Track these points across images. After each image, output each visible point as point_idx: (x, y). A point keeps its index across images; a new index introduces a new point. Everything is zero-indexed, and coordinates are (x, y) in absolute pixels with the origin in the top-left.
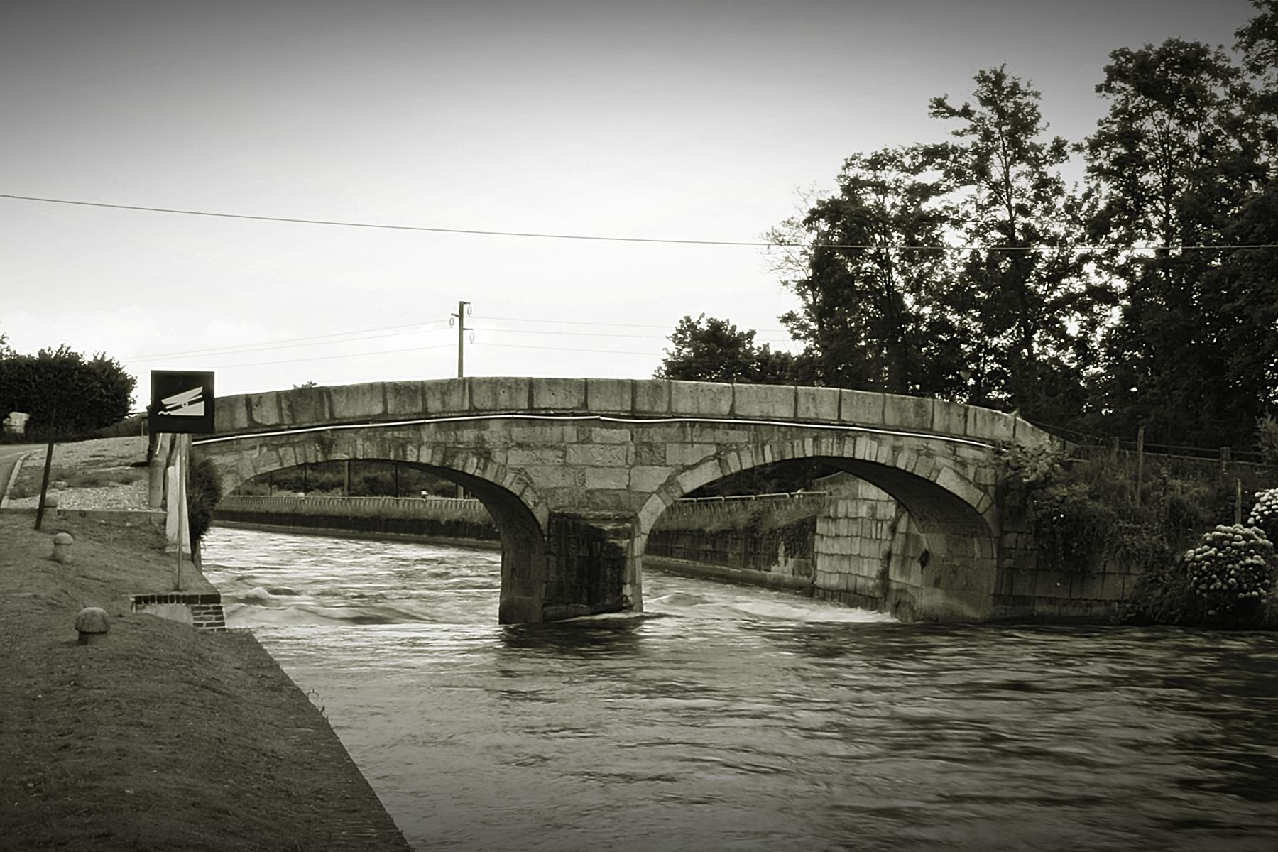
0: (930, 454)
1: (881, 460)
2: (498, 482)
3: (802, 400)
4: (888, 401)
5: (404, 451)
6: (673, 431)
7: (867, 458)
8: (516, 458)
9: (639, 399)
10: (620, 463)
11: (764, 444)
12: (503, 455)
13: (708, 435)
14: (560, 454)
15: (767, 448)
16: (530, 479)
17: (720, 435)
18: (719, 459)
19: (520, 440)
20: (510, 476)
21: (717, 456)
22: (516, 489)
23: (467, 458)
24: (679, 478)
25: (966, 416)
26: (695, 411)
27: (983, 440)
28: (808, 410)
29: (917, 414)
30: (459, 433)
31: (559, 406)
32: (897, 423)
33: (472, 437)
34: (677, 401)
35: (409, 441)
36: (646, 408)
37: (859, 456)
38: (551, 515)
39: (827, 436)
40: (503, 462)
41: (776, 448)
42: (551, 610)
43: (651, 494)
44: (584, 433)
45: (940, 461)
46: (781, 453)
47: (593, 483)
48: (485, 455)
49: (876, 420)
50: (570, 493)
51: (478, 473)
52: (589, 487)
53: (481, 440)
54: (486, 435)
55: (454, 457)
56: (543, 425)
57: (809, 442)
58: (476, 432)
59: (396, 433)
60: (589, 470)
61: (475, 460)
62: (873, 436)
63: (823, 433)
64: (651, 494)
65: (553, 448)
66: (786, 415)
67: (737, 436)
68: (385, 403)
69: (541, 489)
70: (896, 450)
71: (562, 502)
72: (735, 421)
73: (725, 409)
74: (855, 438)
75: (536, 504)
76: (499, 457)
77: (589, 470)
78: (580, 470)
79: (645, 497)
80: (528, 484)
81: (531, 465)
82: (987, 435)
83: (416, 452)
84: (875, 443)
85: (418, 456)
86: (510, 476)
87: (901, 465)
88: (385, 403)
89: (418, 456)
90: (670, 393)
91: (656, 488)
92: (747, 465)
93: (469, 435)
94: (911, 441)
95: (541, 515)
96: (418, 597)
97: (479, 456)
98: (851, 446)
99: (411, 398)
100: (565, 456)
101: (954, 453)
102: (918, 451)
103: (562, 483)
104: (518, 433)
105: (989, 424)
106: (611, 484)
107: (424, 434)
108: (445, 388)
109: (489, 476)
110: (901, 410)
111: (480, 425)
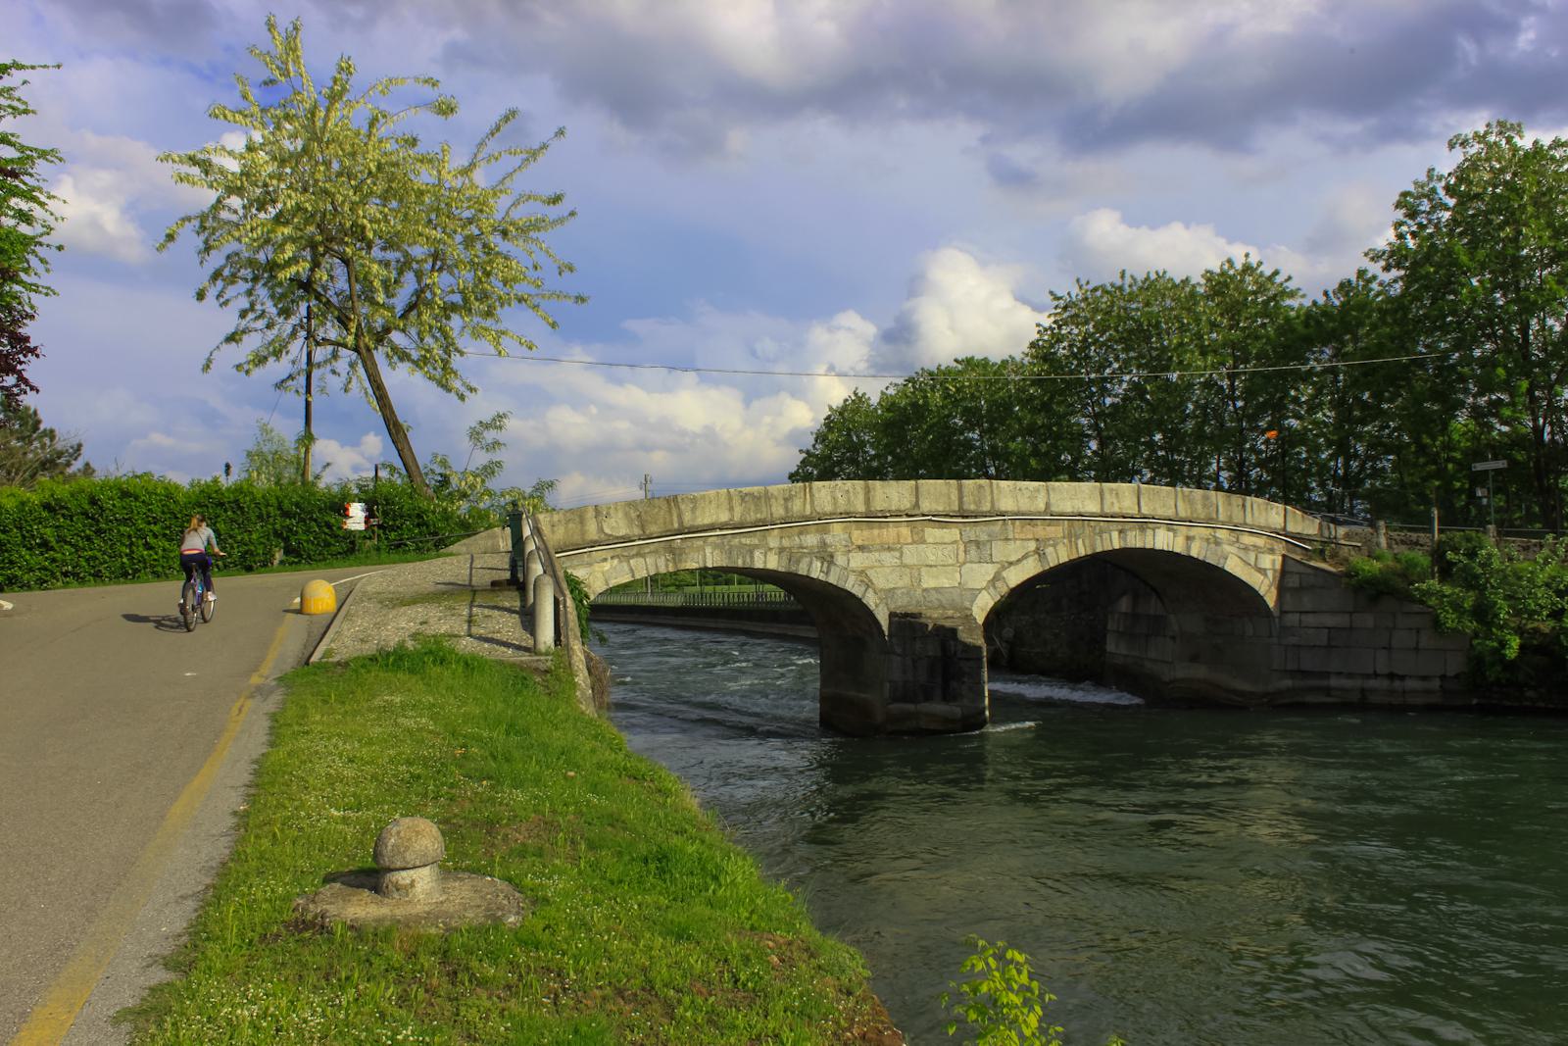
0: (1217, 543)
1: (1177, 550)
2: (841, 585)
3: (1107, 496)
4: (1180, 495)
5: (752, 558)
6: (997, 527)
7: (1166, 549)
8: (858, 560)
9: (965, 499)
10: (950, 561)
11: (1077, 538)
12: (845, 558)
13: (1029, 531)
14: (897, 554)
15: (1080, 542)
16: (870, 581)
17: (1041, 531)
18: (1039, 553)
19: (860, 543)
20: (852, 579)
21: (1037, 551)
22: (857, 591)
23: (811, 563)
24: (1004, 574)
25: (1244, 506)
26: (1016, 509)
27: (1261, 528)
28: (1113, 506)
29: (1204, 506)
30: (802, 537)
31: (893, 508)
32: (1189, 514)
33: (815, 543)
34: (998, 500)
35: (756, 547)
36: (972, 507)
37: (1159, 546)
38: (892, 615)
39: (1130, 530)
40: (845, 565)
41: (1087, 542)
42: (896, 707)
43: (980, 590)
44: (917, 534)
45: (1227, 548)
46: (1093, 545)
47: (929, 582)
48: (828, 559)
49: (1170, 513)
50: (908, 593)
51: (822, 577)
52: (925, 586)
53: (824, 544)
54: (829, 539)
55: (798, 562)
56: (880, 528)
57: (1115, 534)
58: (819, 537)
59: (743, 540)
60: (923, 569)
61: (819, 564)
62: (1170, 528)
63: (1127, 526)
64: (980, 590)
65: (889, 549)
66: (1094, 510)
67: (1057, 531)
68: (731, 509)
69: (881, 590)
70: (1189, 538)
71: (901, 604)
72: (1051, 517)
73: (1042, 506)
74: (1154, 530)
75: (877, 606)
76: (840, 560)
77: (923, 569)
78: (915, 571)
79: (975, 593)
80: (868, 584)
81: (872, 568)
82: (1263, 523)
83: (762, 557)
84: (1171, 534)
85: (765, 562)
86: (852, 579)
87: (1194, 553)
88: (731, 509)
89: (765, 562)
90: (992, 492)
91: (984, 584)
92: (1064, 559)
93: (811, 540)
94: (1199, 532)
95: (883, 618)
96: (1500, 963)
97: (823, 560)
98: (1151, 537)
99: (756, 505)
100: (901, 556)
101: (1238, 541)
102: (1208, 540)
103: (900, 584)
104: (859, 536)
105: (1264, 514)
106: (945, 583)
107: (770, 539)
108: (923, 477)
109: (832, 580)
110: (1190, 501)
111: (824, 529)
